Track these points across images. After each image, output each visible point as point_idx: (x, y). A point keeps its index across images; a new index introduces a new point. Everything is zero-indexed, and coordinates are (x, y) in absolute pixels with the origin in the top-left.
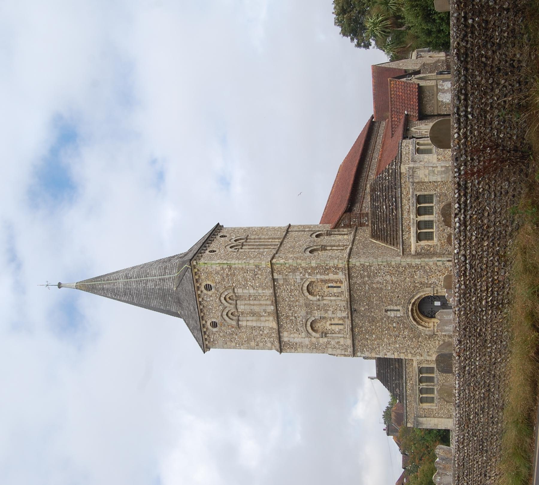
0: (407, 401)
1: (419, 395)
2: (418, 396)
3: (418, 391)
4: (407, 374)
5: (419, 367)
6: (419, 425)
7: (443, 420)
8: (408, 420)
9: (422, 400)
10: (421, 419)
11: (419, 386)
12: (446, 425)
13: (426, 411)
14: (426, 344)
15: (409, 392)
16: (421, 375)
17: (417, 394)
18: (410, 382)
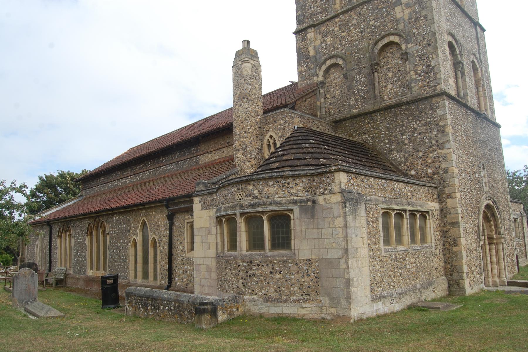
0: (383, 181)
1: (394, 210)
2: (395, 207)
3: (401, 207)
4: (419, 187)
5: (428, 212)
6: (353, 204)
7: (366, 271)
8: (353, 175)
9: (386, 214)
10: (362, 210)
11: (408, 210)
12: (357, 281)
13: (374, 226)
14: (471, 226)
15: (396, 185)
16: (418, 215)
17: (397, 204)
18: (409, 191)
